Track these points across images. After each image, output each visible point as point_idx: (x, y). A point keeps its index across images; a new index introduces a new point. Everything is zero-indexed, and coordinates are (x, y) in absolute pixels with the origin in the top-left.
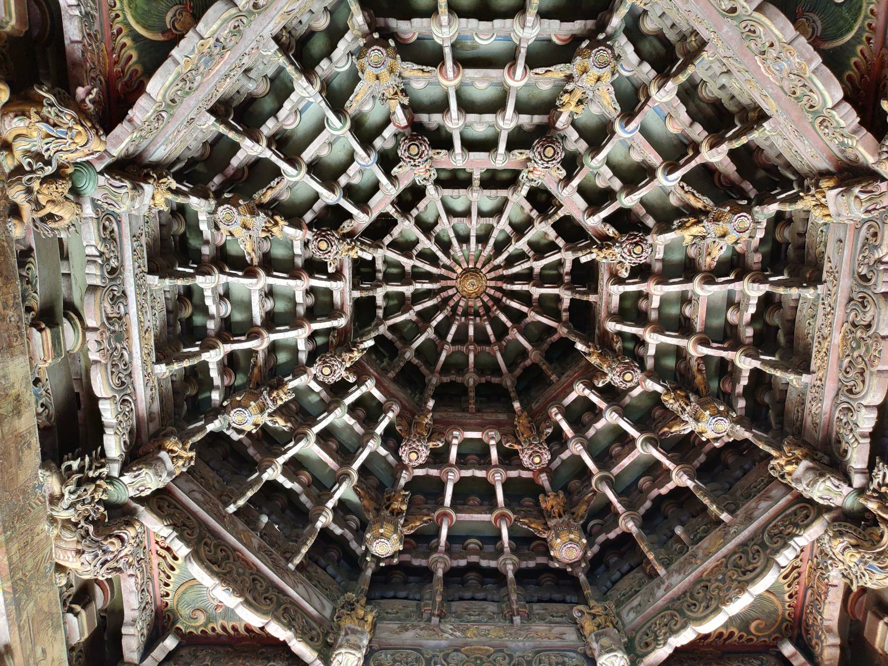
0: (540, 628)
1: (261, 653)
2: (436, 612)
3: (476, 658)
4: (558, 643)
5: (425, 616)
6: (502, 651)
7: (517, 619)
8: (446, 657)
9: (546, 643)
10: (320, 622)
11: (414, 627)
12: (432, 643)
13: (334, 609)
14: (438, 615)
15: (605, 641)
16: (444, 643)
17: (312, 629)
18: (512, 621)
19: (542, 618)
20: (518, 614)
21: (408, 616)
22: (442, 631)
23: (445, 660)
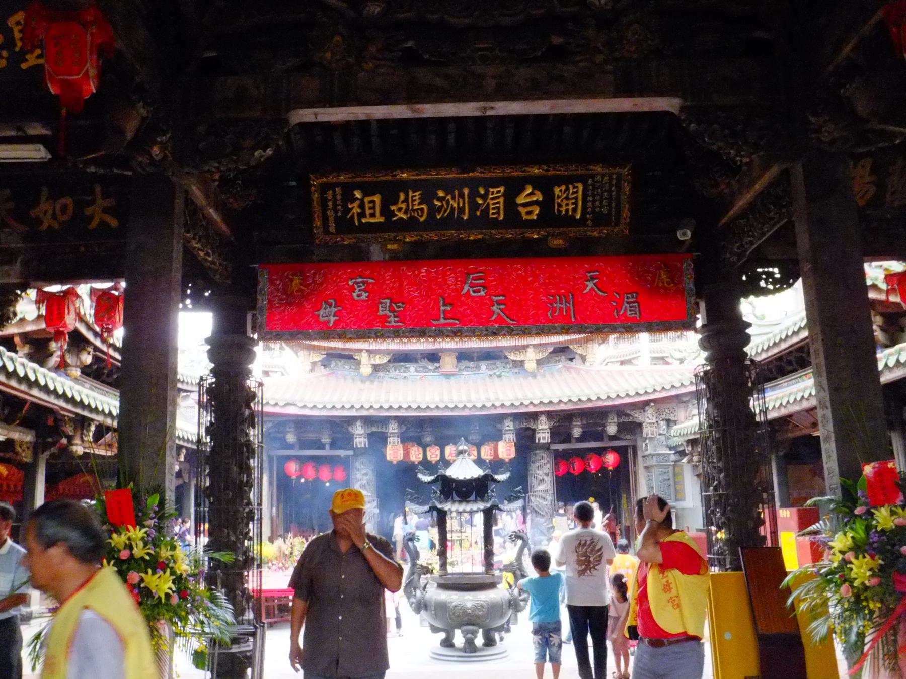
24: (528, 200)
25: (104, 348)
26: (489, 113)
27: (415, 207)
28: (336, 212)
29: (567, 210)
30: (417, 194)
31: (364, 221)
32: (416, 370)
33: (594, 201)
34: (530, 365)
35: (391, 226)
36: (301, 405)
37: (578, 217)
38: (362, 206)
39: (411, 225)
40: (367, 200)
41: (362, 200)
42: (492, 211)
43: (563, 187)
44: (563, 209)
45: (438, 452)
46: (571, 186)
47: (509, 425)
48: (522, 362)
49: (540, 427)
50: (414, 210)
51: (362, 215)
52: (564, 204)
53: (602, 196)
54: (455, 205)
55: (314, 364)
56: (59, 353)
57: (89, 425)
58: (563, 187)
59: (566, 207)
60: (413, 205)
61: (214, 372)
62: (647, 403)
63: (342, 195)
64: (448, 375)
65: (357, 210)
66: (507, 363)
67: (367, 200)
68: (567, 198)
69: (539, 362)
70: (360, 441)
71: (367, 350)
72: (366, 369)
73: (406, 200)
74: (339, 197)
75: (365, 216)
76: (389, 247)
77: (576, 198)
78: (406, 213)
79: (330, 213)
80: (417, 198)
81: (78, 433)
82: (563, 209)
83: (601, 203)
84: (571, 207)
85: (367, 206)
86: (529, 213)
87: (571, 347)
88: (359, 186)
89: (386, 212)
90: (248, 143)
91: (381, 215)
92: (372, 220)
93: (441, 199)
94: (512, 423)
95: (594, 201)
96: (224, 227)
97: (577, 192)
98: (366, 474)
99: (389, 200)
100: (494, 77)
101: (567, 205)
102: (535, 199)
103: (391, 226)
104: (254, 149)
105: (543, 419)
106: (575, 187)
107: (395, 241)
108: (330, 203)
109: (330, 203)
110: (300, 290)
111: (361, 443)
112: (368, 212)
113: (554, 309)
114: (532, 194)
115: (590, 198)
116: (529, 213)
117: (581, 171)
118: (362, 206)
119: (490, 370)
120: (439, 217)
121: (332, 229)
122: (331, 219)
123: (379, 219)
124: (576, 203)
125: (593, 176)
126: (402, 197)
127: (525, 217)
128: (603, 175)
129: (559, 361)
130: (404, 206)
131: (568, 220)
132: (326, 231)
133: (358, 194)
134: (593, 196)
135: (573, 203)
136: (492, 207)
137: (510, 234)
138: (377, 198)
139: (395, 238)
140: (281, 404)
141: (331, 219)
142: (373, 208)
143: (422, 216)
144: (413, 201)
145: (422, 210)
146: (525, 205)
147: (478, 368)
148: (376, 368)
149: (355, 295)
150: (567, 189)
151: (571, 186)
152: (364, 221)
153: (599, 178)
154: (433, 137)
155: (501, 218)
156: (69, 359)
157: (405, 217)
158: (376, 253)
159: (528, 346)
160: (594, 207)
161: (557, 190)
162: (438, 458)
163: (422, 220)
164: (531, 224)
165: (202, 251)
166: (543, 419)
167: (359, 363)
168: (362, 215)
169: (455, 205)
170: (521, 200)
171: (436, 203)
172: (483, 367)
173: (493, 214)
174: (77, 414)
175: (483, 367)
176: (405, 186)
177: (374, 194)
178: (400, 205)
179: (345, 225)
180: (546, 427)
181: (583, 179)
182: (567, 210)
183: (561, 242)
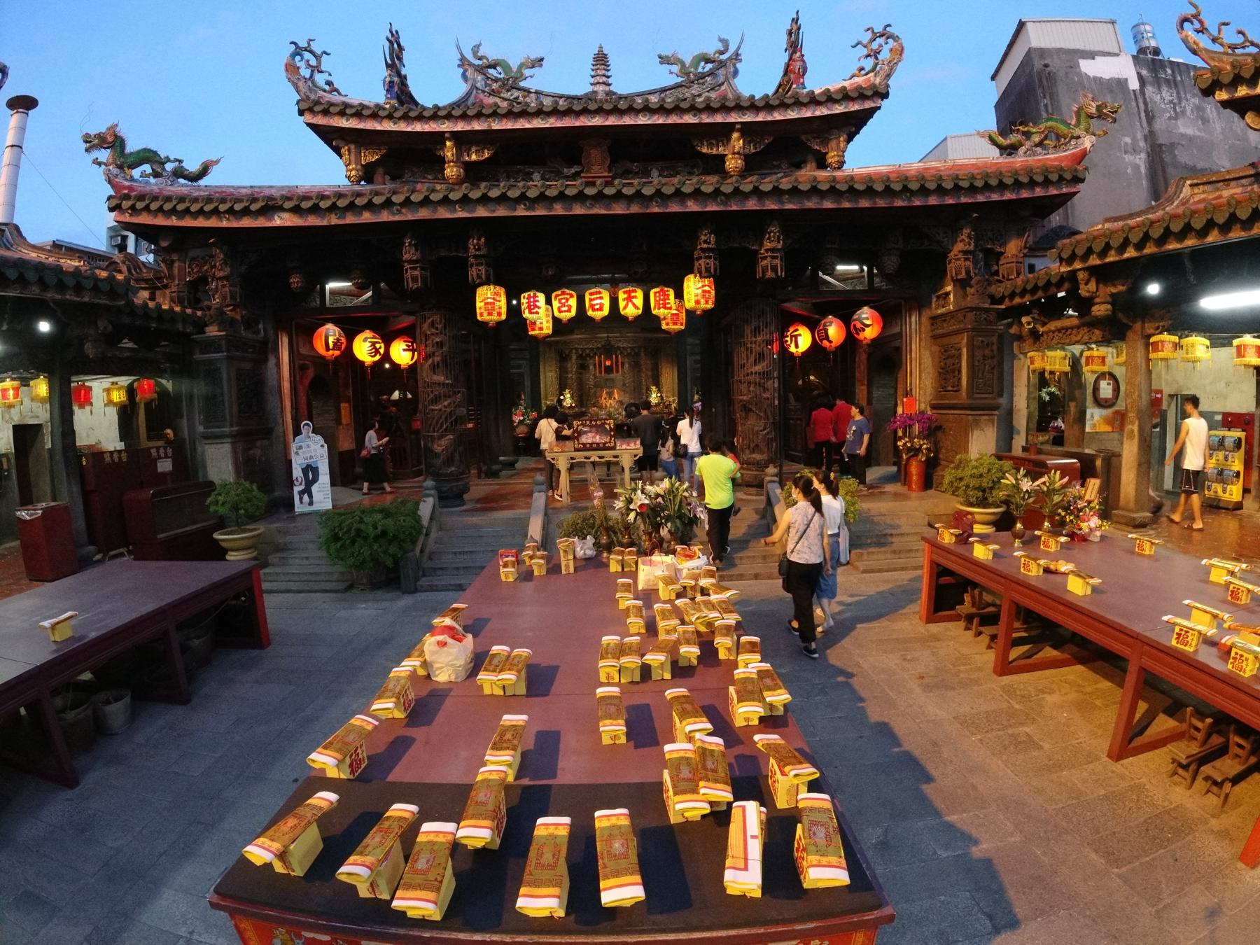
32: (543, 178)
45: (573, 302)
47: (706, 239)
48: (721, 159)
49: (768, 245)
62: (961, 211)
66: (693, 167)
69: (748, 159)
70: (413, 276)
71: (456, 136)
87: (803, 137)
94: (713, 239)
98: (440, 345)
105: (774, 229)
111: (414, 279)
129: (779, 167)
159: (730, 127)
162: (573, 312)
166: (774, 229)
175: (655, 173)
180: (780, 246)
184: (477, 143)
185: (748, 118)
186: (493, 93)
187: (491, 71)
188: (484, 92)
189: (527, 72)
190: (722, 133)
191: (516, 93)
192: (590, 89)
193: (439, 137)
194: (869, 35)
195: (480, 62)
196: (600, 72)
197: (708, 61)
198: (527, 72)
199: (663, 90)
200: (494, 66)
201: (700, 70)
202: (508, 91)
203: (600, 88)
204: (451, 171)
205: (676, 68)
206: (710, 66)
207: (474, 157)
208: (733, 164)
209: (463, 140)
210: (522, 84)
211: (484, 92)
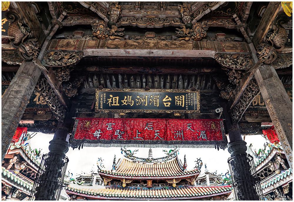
0: (169, 12)
1: (91, 18)
2: (139, 7)
3: (150, 19)
4: (173, 15)
5: (136, 9)
6: (157, 17)
7: (162, 9)
8: (142, 18)
9: (169, 15)
10: (106, 9)
11: (133, 11)
12: (138, 15)
13: (109, 6)
14: (140, 8)
15: (185, 13)
16: (141, 15)
17: (103, 10)
18: (161, 10)
19: (170, 10)
20: (163, 8)
21: (131, 9)
22: (141, 12)
23: (142, 19)
24: (167, 100)
25: (31, 164)
26: (151, 55)
27: (130, 101)
28: (103, 102)
29: (179, 104)
30: (130, 97)
31: (112, 105)
33: (188, 101)
34: (174, 185)
35: (121, 107)
36: (101, 195)
37: (183, 106)
38: (112, 100)
39: (128, 107)
40: (114, 98)
41: (112, 98)
42: (154, 104)
43: (178, 97)
44: (178, 104)
46: (180, 97)
50: (129, 102)
51: (112, 103)
52: (178, 102)
53: (191, 100)
54: (143, 101)
55: (108, 183)
56: (12, 164)
57: (16, 191)
58: (178, 97)
59: (179, 103)
60: (129, 100)
61: (50, 154)
63: (106, 96)
64: (149, 188)
65: (110, 101)
67: (114, 98)
68: (179, 100)
71: (125, 179)
72: (124, 185)
73: (127, 99)
74: (105, 97)
75: (113, 104)
76: (121, 114)
77: (182, 100)
78: (126, 103)
79: (101, 102)
80: (130, 98)
81: (11, 194)
82: (178, 104)
83: (190, 102)
84: (180, 103)
85: (114, 100)
86: (167, 105)
88: (111, 93)
89: (120, 102)
90: (66, 57)
91: (118, 104)
92: (115, 105)
93: (138, 99)
95: (188, 101)
96: (63, 101)
97: (182, 98)
99: (121, 98)
100: (153, 43)
101: (179, 102)
102: (169, 100)
103: (121, 107)
104: (68, 59)
106: (182, 97)
107: (123, 112)
108: (102, 99)
109: (102, 99)
110: (89, 126)
112: (114, 102)
113: (176, 135)
114: (168, 98)
115: (187, 100)
116: (167, 105)
117: (183, 91)
118: (112, 100)
119: (162, 186)
120: (137, 105)
121: (102, 107)
122: (102, 104)
123: (117, 105)
124: (182, 102)
125: (187, 93)
126: (126, 97)
127: (165, 106)
128: (191, 93)
130: (126, 101)
131: (180, 108)
132: (99, 108)
133: (111, 96)
134: (188, 100)
135: (181, 102)
136: (155, 102)
137: (161, 111)
138: (117, 98)
139: (122, 111)
140: (95, 194)
141: (102, 104)
142: (116, 101)
143: (132, 104)
144: (129, 99)
145: (132, 102)
146: (166, 102)
147: (159, 186)
148: (127, 185)
149: (107, 128)
150: (179, 97)
151: (180, 97)
152: (112, 105)
153: (189, 94)
154: (138, 83)
155: (158, 106)
156: (16, 166)
157: (126, 104)
158: (116, 116)
160: (188, 104)
161: (176, 97)
163: (131, 105)
164: (168, 108)
165: (51, 104)
167: (122, 183)
168: (112, 103)
169: (143, 101)
170: (164, 100)
171: (136, 100)
172: (160, 185)
173: (155, 104)
174: (13, 186)
175: (160, 185)
176: (126, 94)
177: (116, 97)
178: (125, 100)
179: (106, 106)
181: (184, 94)
182: (179, 104)
183: (179, 114)
184: (129, 180)
185: (176, 177)
186: (128, 157)
187: (127, 152)
188: (125, 157)
189: (135, 153)
190: (172, 179)
191: (132, 157)
192: (148, 157)
193: (123, 179)
194: (197, 160)
195: (125, 150)
196: (150, 154)
197: (173, 151)
198: (135, 153)
199: (163, 158)
200: (128, 151)
201: (171, 153)
202: (131, 157)
203: (150, 157)
204: (124, 185)
205: (166, 153)
206: (173, 152)
207: (128, 183)
208: (174, 185)
209: (126, 179)
210: (133, 155)
211: (125, 157)
